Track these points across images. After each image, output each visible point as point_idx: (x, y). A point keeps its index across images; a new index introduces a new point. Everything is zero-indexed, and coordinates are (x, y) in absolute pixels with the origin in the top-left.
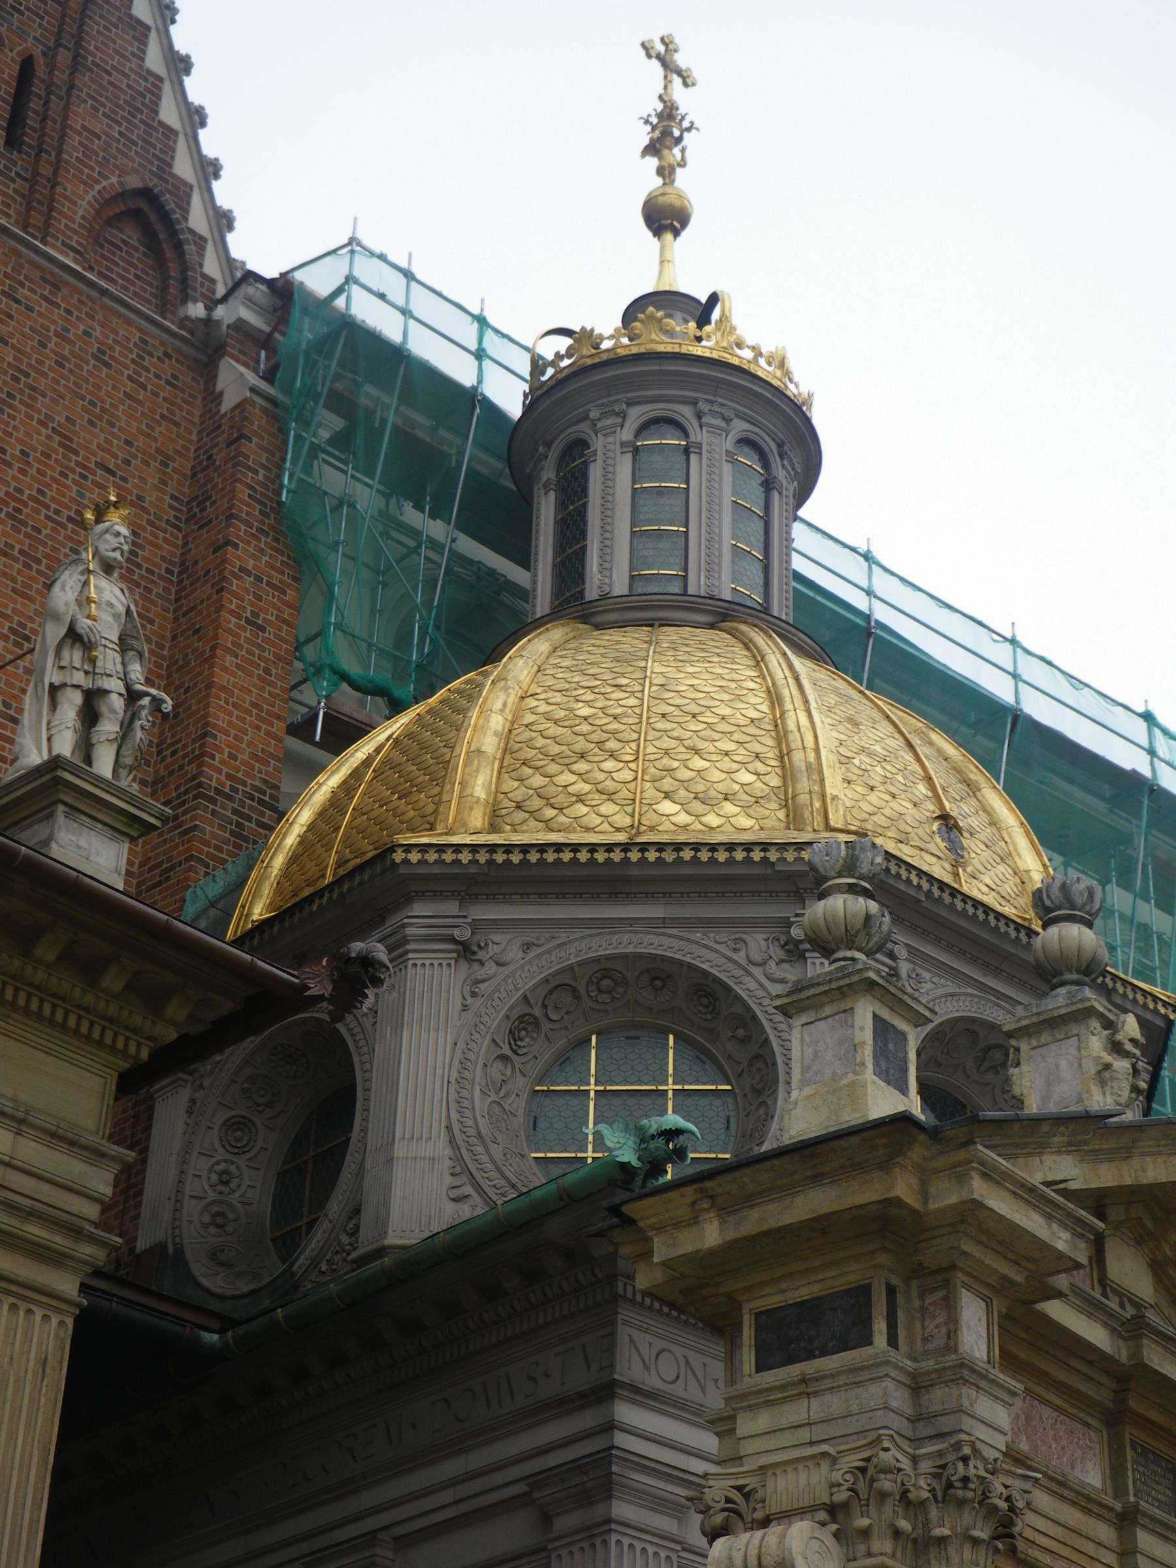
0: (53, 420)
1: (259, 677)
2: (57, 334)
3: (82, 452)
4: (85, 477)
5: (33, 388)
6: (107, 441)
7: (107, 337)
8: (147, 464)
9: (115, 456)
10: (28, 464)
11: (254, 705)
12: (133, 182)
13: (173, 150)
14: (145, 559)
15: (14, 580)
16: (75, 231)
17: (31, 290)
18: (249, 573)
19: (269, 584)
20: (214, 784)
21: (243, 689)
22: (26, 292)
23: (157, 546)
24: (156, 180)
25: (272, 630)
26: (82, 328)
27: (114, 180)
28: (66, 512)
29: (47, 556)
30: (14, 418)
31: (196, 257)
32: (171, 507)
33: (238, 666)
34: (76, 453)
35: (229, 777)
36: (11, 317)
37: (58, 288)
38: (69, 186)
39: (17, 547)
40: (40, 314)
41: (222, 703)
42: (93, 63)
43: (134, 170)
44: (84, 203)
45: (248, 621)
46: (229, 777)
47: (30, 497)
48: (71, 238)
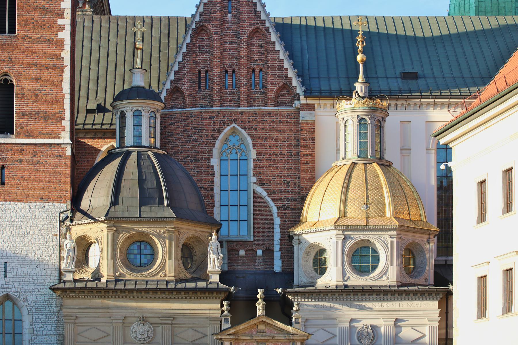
0: (273, 138)
2: (272, 122)
4: (281, 145)
5: (269, 134)
8: (291, 136)
12: (281, 84)
13: (287, 72)
14: (294, 154)
15: (272, 170)
16: (272, 101)
17: (267, 117)
18: (305, 155)
21: (306, 176)
23: (296, 151)
27: (277, 86)
29: (276, 163)
34: (279, 142)
35: (306, 193)
43: (281, 82)
44: (273, 94)
46: (306, 193)
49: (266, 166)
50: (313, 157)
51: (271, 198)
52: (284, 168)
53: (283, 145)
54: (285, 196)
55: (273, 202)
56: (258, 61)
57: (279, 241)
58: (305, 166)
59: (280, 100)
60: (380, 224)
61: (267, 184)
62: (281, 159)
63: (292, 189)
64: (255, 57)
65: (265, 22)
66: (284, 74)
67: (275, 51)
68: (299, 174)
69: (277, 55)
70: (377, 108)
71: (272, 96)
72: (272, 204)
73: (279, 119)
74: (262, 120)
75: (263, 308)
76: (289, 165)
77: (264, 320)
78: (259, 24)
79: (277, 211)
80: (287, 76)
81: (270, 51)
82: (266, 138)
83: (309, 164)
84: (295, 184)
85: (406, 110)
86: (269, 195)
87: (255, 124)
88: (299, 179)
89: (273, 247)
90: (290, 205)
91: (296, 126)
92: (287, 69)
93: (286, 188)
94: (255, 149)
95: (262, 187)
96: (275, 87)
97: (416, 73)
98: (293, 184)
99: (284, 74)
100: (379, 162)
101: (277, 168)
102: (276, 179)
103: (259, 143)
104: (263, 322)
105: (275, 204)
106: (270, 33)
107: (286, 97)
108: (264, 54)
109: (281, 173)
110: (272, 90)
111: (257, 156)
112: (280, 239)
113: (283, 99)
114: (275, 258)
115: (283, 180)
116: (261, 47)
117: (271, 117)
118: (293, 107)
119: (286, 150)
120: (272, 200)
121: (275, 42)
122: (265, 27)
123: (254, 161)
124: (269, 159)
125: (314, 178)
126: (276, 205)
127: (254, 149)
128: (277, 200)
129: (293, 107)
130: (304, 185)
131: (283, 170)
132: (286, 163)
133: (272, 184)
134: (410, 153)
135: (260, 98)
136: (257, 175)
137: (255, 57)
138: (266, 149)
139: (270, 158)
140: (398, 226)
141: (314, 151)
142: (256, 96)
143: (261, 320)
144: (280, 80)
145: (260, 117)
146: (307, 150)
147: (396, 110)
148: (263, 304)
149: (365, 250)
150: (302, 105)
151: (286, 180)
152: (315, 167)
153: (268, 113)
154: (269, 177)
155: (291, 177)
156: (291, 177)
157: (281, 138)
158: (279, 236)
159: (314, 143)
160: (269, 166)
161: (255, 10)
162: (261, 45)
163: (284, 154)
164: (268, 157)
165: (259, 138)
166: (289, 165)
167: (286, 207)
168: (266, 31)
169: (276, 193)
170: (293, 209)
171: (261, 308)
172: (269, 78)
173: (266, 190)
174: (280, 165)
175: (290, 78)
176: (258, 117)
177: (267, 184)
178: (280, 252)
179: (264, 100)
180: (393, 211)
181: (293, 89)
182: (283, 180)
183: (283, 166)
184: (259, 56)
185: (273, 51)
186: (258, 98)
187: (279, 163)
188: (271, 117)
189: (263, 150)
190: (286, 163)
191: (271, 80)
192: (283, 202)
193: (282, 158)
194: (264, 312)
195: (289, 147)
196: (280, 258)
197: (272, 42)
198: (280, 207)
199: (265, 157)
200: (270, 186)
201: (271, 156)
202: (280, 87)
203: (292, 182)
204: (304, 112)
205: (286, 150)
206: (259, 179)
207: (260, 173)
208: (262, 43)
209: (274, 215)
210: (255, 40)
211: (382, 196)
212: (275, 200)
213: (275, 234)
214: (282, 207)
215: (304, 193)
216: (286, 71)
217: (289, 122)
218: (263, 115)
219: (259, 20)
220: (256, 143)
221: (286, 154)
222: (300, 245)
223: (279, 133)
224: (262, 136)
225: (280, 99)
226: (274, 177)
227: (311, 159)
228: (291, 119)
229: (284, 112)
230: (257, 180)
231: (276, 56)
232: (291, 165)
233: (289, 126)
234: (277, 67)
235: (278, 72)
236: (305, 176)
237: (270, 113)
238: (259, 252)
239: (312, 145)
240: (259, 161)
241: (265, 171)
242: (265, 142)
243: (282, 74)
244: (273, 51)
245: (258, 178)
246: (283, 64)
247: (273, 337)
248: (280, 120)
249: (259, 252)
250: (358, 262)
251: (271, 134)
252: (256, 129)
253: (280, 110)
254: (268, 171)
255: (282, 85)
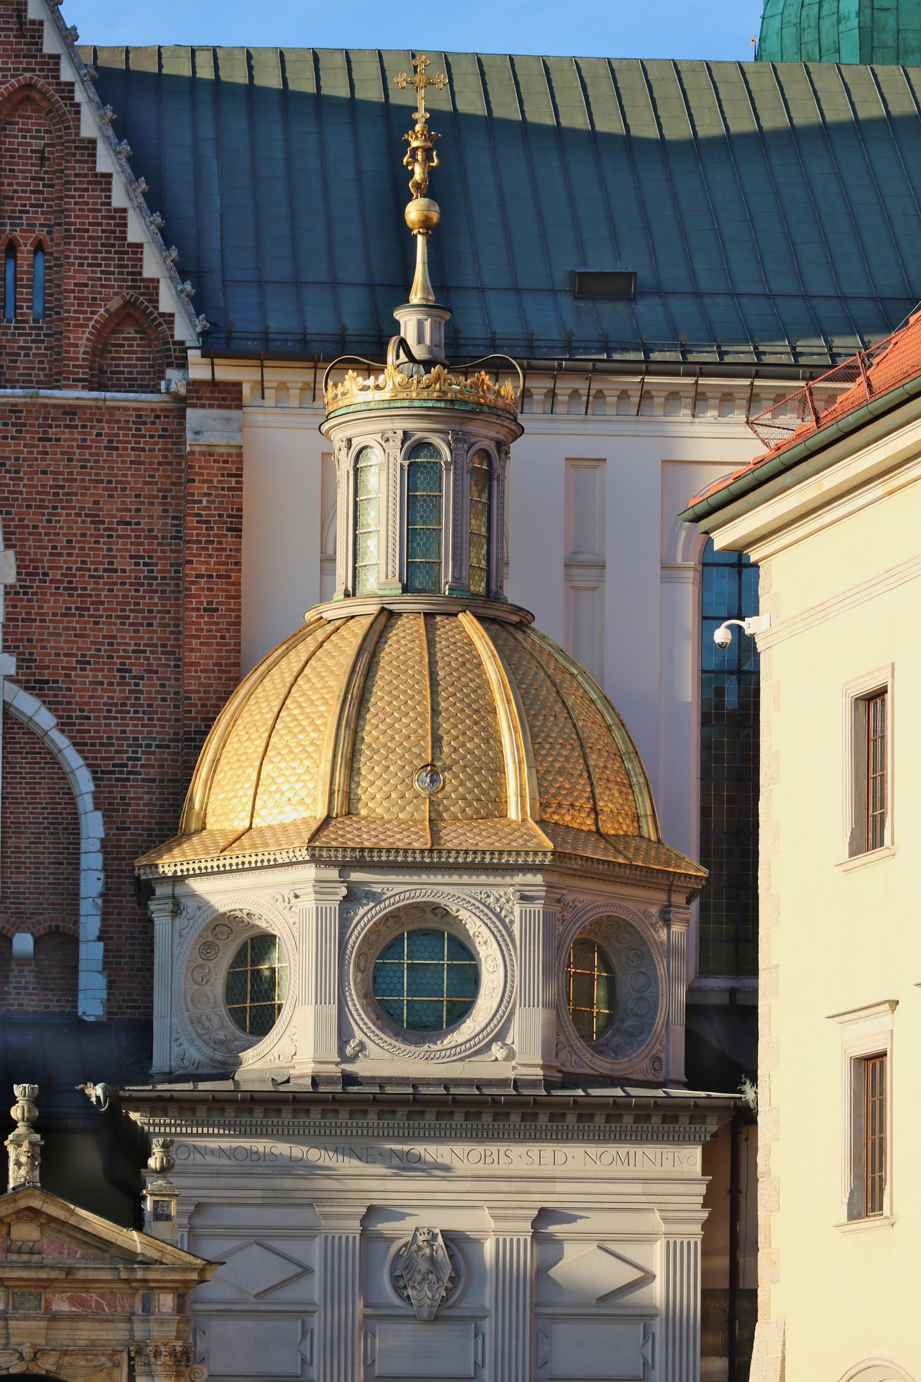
1: (218, 644)
2: (79, 447)
3: (107, 520)
4: (110, 536)
6: (123, 503)
7: (113, 429)
8: (152, 504)
9: (130, 510)
10: (74, 548)
11: (215, 665)
12: (115, 304)
13: (141, 260)
14: (159, 571)
15: (75, 629)
16: (80, 367)
17: (58, 426)
18: (202, 576)
19: (218, 577)
20: (193, 729)
21: (206, 657)
22: (54, 430)
23: (169, 558)
24: (131, 292)
25: (223, 608)
26: (95, 432)
27: (102, 311)
28: (102, 567)
29: (92, 603)
30: (58, 522)
31: (168, 333)
32: (173, 525)
33: (201, 644)
34: (103, 522)
35: (203, 719)
36: (46, 453)
37: (75, 413)
38: (71, 336)
39: (73, 606)
40: (66, 440)
41: (193, 674)
42: (76, 230)
43: (115, 294)
44: (84, 342)
45: (205, 610)
47: (78, 569)
48: (78, 373)
49: (55, 615)
50: (233, 584)
51: (70, 738)
52: (123, 624)
53: (119, 537)
54: (124, 732)
55: (80, 752)
56: (27, 212)
57: (99, 901)
58: (202, 617)
59: (110, 366)
60: (482, 846)
61: (56, 682)
62: (111, 590)
63: (150, 706)
64: (19, 198)
65: (58, 64)
66: (126, 266)
67: (96, 175)
68: (178, 646)
69: (102, 190)
70: (479, 404)
71: (82, 350)
72: (73, 759)
73: (107, 435)
74: (40, 439)
75: (32, 1158)
76: (142, 611)
77: (36, 1203)
78: (33, 70)
79: (92, 788)
80: (140, 274)
81: (76, 175)
82: (55, 508)
83: (216, 610)
84: (163, 686)
85: (589, 417)
86: (64, 726)
87: (14, 452)
88: (176, 666)
89: (76, 923)
90: (143, 766)
91: (170, 464)
92: (140, 246)
93: (129, 698)
94: (14, 546)
95: (38, 696)
96: (93, 313)
97: (629, 276)
98: (154, 686)
99: (126, 266)
100: (481, 611)
101: (96, 623)
102: (89, 663)
103: (27, 527)
104: (33, 1214)
105: (86, 758)
106: (78, 105)
107: (135, 352)
108: (52, 186)
109: (111, 644)
110: (82, 326)
111: (18, 573)
112: (102, 895)
113: (122, 359)
114: (82, 966)
115: (119, 670)
116: (43, 158)
117: (76, 427)
118: (159, 391)
119: (131, 557)
120: (75, 744)
121: (93, 142)
122: (59, 84)
123: (7, 593)
124: (65, 589)
125: (234, 665)
126: (88, 766)
127: (7, 547)
128: (93, 745)
129: (159, 391)
130: (198, 692)
131: (119, 631)
132: (129, 604)
133: (74, 682)
134: (602, 579)
135: (35, 355)
136: (17, 647)
137: (19, 198)
138: (55, 548)
139: (70, 582)
140: (550, 857)
141: (238, 563)
142: (20, 348)
143: (23, 1204)
144: (112, 287)
145: (33, 425)
146: (210, 556)
147: (549, 416)
148: (32, 1144)
149: (426, 943)
150: (194, 386)
151: (129, 671)
152: (239, 624)
153: (65, 413)
154: (66, 655)
155: (147, 659)
156: (147, 659)
157: (111, 508)
158: (100, 883)
159: (237, 531)
160: (63, 615)
161: (19, 17)
162: (43, 152)
163: (124, 571)
164: (62, 582)
165: (29, 507)
166: (142, 611)
167: (129, 773)
168: (63, 98)
169: (89, 718)
170: (153, 781)
171: (23, 1159)
172: (68, 277)
173: (51, 706)
174: (105, 610)
175: (152, 280)
176: (24, 425)
177: (56, 682)
178: (101, 945)
179: (50, 362)
180: (532, 799)
181: (160, 324)
182: (119, 670)
183: (117, 617)
184: (32, 192)
185: (86, 175)
186: (27, 355)
187: (102, 603)
188: (76, 427)
189: (44, 554)
190: (129, 604)
191: (76, 285)
192: (117, 752)
193: (115, 584)
194: (37, 1173)
195: (142, 544)
196: (99, 966)
197: (82, 141)
198: (103, 772)
199: (52, 581)
200: (69, 689)
201: (74, 576)
202: (112, 315)
203: (150, 679)
204: (200, 412)
205: (131, 557)
206: (24, 662)
207: (30, 640)
208: (46, 145)
209: (79, 800)
210: (20, 130)
211: (492, 738)
212: (85, 744)
213: (83, 875)
214: (113, 772)
215: (196, 719)
216: (135, 253)
217: (143, 450)
218: (45, 419)
219: (35, 57)
220: (16, 526)
221: (132, 571)
222: (177, 920)
223: (104, 489)
224: (42, 500)
225: (113, 359)
226: (84, 656)
227: (223, 590)
228: (152, 437)
229: (126, 409)
230: (19, 667)
231: (100, 197)
232: (150, 611)
233: (143, 463)
234: (100, 238)
235: (103, 259)
236: (201, 657)
237: (71, 411)
238: (23, 943)
239: (230, 538)
240: (26, 593)
241: (50, 634)
242: (49, 521)
243: (119, 266)
244: (86, 175)
245: (23, 660)
246: (125, 225)
247: (70, 1271)
248: (110, 442)
249: (23, 943)
250: (399, 987)
251: (76, 494)
252: (17, 472)
253: (108, 403)
254: (59, 635)
255: (121, 308)
